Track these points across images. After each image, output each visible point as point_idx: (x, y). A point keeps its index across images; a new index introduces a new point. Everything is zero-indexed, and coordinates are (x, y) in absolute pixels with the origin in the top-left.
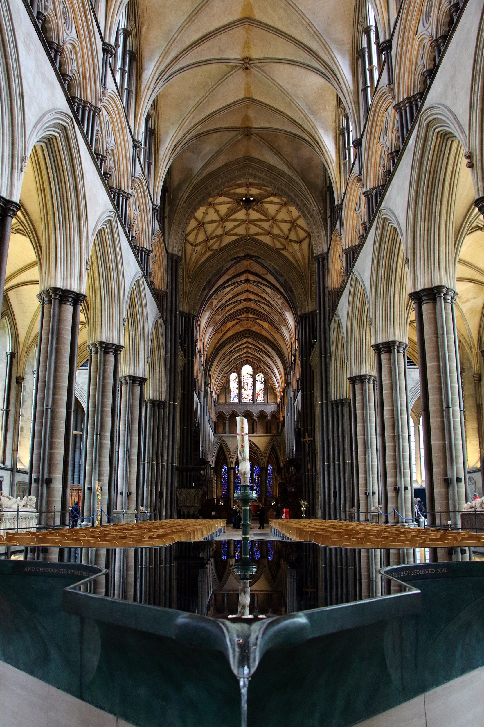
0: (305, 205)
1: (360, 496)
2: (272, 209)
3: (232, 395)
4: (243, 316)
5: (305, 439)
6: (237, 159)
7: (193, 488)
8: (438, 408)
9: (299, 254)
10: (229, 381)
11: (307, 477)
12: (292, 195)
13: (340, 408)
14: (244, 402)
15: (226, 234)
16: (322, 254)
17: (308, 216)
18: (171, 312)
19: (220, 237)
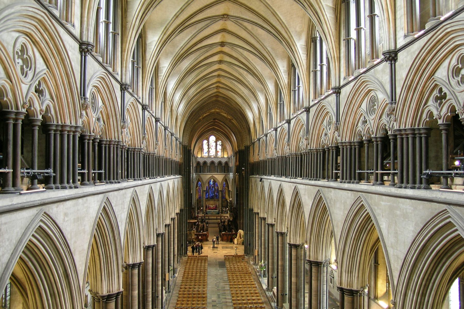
0: (241, 123)
8: (271, 257)
10: (203, 144)
16: (248, 146)
18: (185, 171)
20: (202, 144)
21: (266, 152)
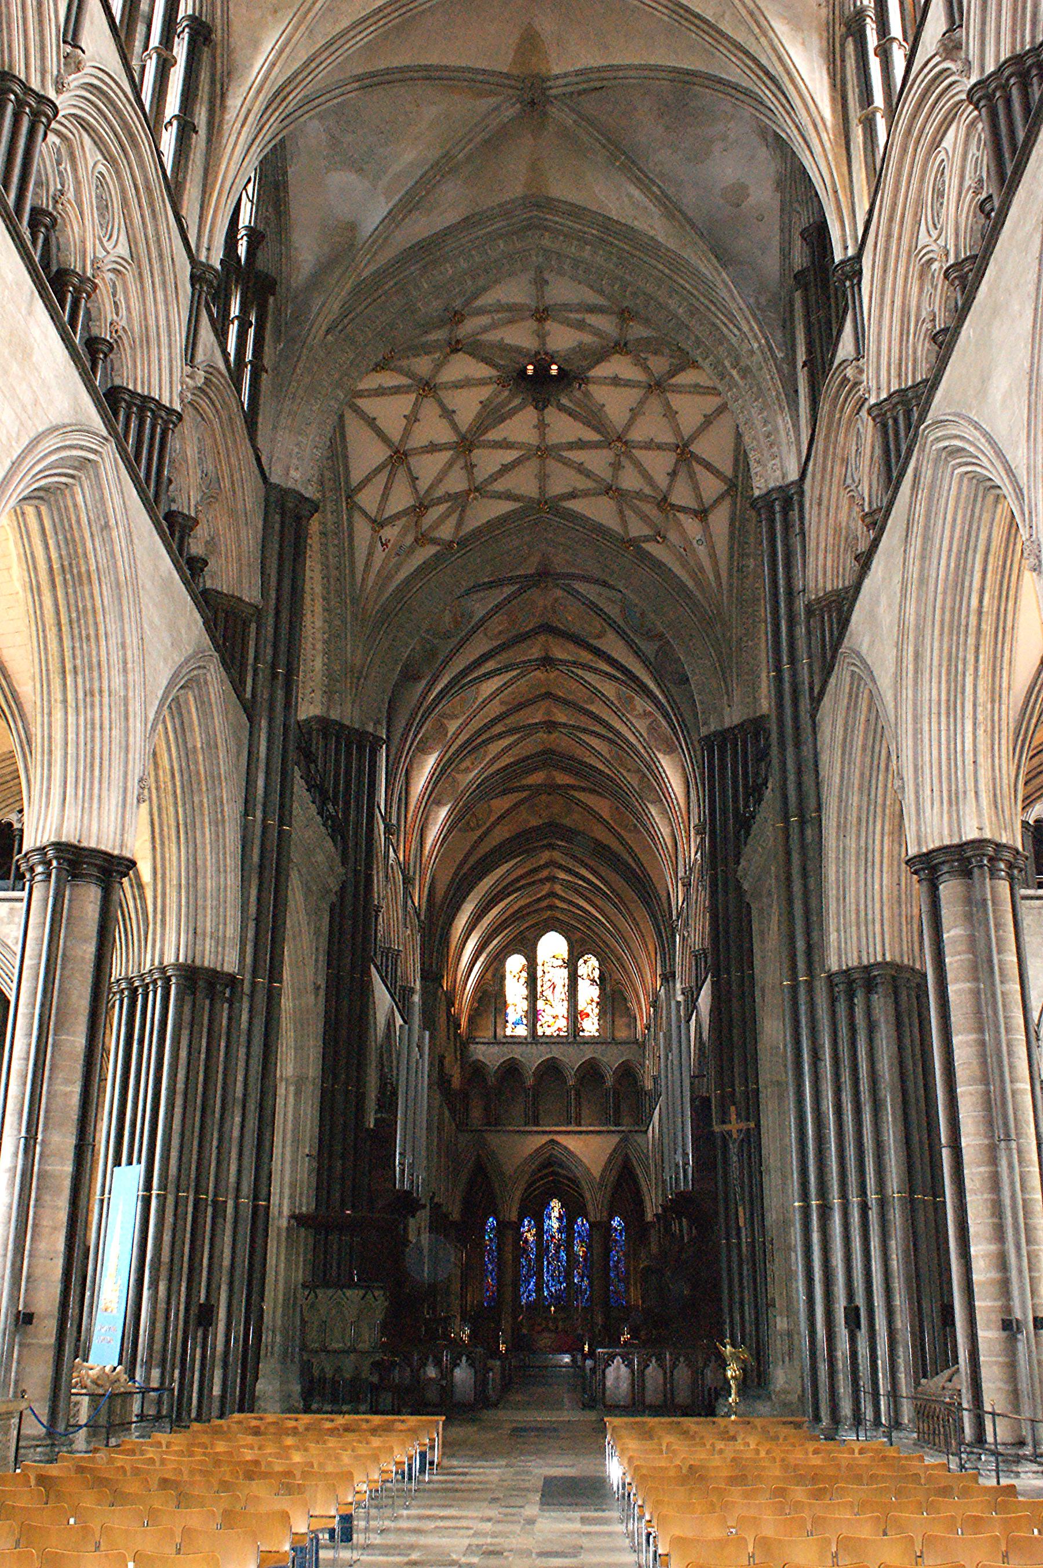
0: (722, 339)
1: (981, 1333)
3: (512, 1017)
4: (537, 778)
5: (726, 1127)
7: (351, 1285)
9: (702, 551)
10: (503, 978)
11: (735, 1252)
13: (859, 1000)
15: (478, 490)
17: (734, 373)
18: (274, 676)
19: (460, 501)
20: (494, 976)
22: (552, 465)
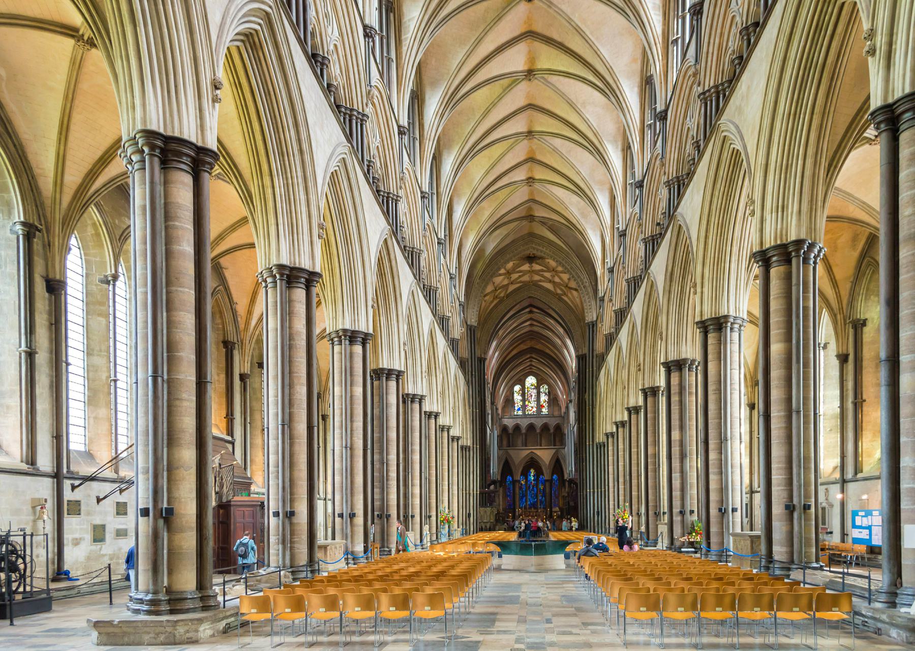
0: (579, 277)
2: (553, 263)
3: (516, 408)
6: (522, 236)
10: (513, 394)
12: (569, 267)
14: (528, 414)
21: (624, 268)
22: (533, 275)
